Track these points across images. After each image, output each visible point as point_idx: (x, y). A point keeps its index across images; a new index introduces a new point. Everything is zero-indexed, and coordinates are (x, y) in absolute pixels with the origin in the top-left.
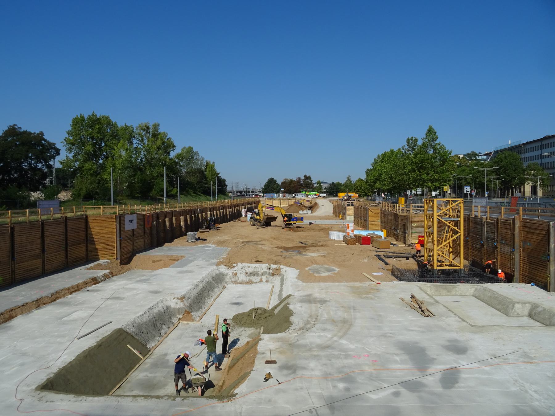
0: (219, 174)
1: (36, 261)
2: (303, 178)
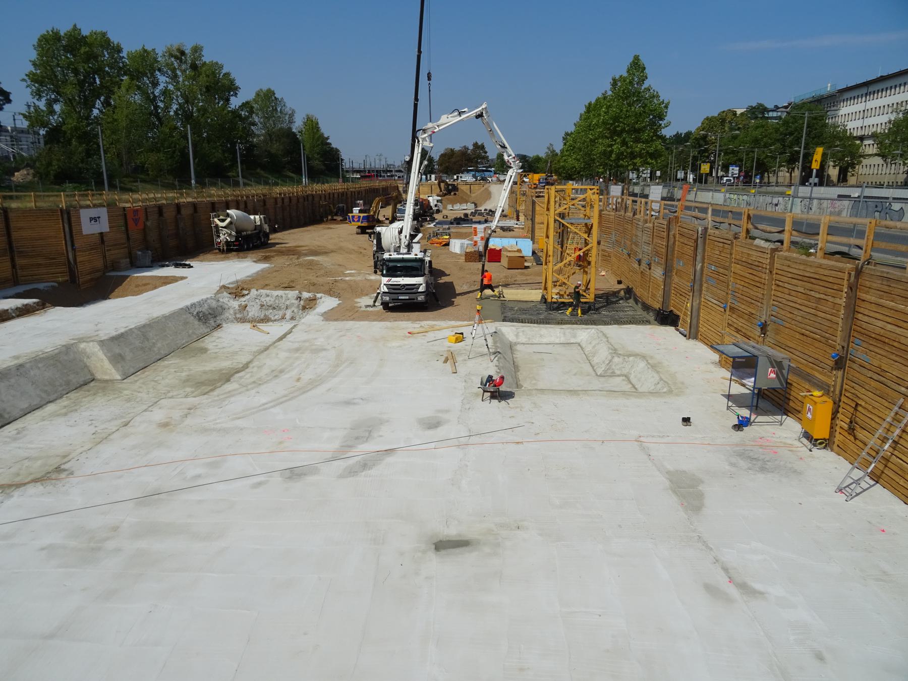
0: (328, 138)
2: (471, 147)
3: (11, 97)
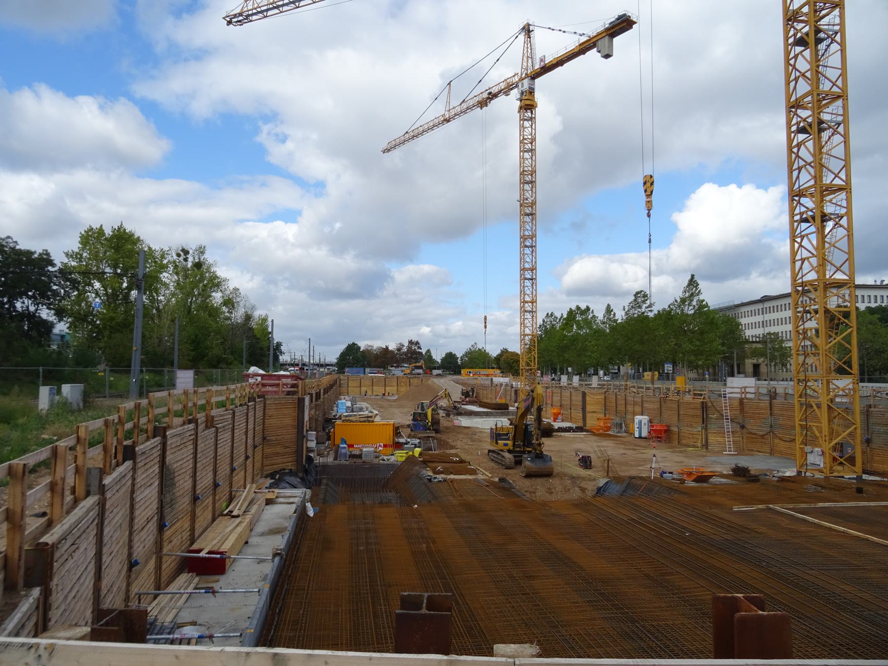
2: (406, 344)
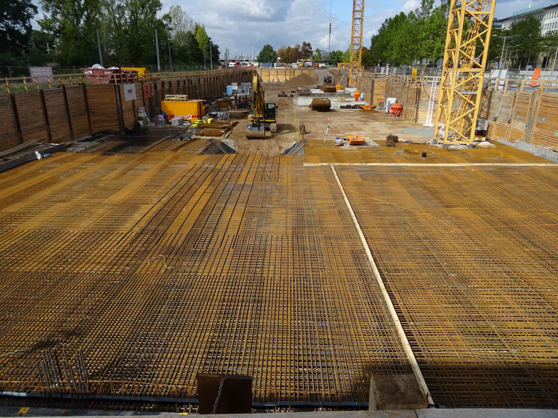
1: (42, 132)
2: (301, 45)
3: (38, 10)
